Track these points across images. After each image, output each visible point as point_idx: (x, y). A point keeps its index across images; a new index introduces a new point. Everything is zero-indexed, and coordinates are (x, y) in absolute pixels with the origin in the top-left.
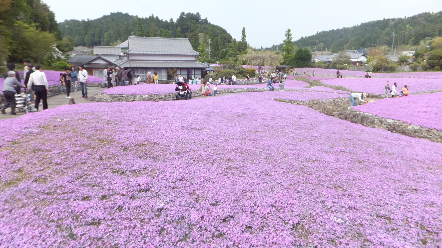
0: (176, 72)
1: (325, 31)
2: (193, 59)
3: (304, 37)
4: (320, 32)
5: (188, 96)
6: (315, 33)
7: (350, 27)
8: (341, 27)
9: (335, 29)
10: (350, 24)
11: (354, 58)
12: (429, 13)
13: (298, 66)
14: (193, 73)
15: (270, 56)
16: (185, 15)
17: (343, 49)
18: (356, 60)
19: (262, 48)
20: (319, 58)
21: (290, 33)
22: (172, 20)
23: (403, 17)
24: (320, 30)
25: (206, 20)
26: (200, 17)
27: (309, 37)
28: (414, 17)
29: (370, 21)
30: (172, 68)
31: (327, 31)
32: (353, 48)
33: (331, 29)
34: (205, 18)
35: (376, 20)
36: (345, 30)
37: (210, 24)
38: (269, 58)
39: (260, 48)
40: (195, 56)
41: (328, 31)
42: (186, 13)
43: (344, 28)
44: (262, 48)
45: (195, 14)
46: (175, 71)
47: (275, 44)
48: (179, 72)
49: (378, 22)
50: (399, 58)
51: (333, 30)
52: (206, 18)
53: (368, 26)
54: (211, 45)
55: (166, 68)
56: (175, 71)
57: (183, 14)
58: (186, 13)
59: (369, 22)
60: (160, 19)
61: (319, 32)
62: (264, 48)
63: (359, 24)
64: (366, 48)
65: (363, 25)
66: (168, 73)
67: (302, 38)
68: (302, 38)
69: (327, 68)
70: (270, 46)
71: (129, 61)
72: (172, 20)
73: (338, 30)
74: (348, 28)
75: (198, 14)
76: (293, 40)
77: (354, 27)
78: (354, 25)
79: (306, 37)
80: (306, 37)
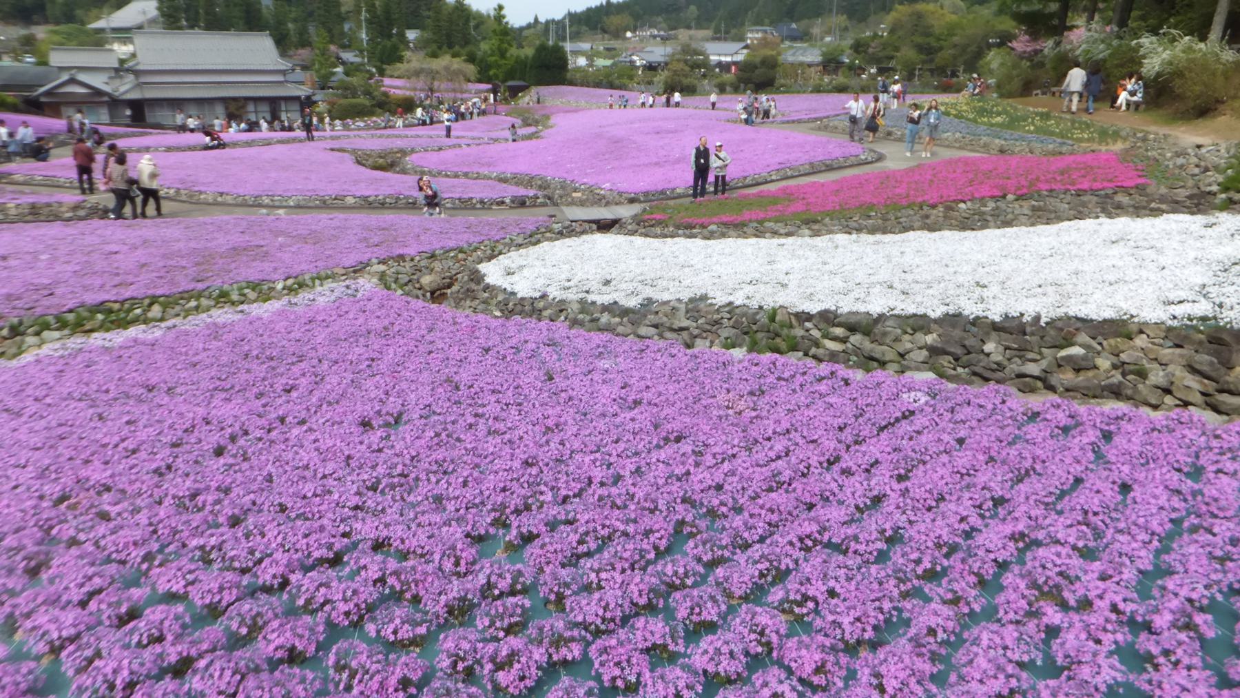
0: (243, 107)
2: (280, 78)
5: (222, 146)
11: (726, 55)
14: (283, 108)
15: (447, 68)
17: (743, 24)
18: (729, 59)
19: (536, 19)
20: (642, 55)
21: (503, 12)
30: (235, 99)
32: (767, 21)
38: (443, 73)
40: (284, 72)
44: (536, 19)
46: (240, 104)
47: (572, 10)
48: (251, 107)
50: (823, 54)
54: (369, 22)
55: (223, 100)
56: (240, 104)
62: (542, 19)
64: (796, 21)
66: (227, 108)
71: (139, 86)
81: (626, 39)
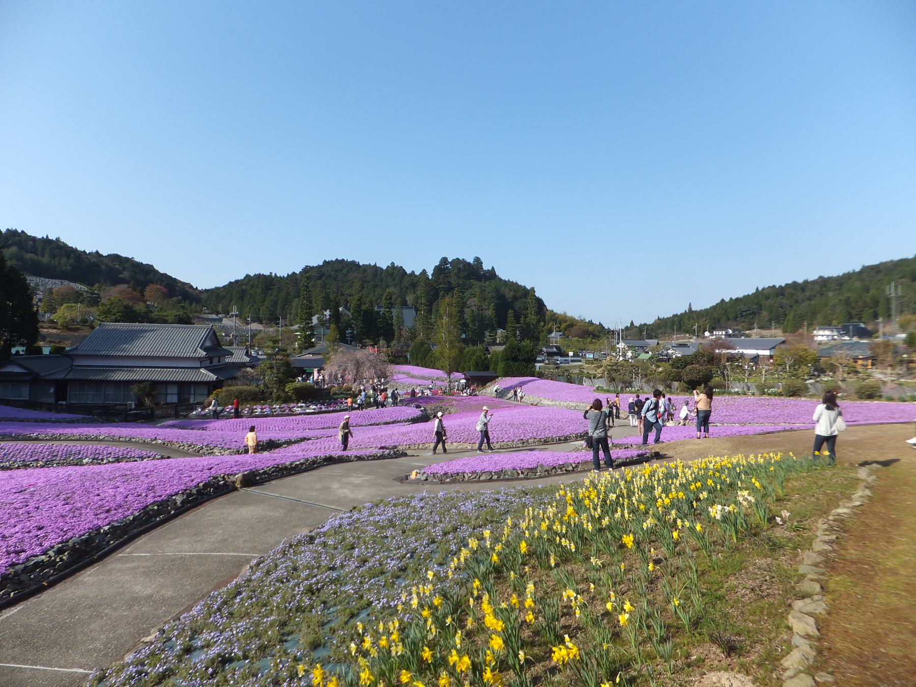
1: (774, 286)
3: (727, 300)
4: (763, 289)
6: (752, 291)
7: (835, 275)
8: (812, 277)
9: (800, 280)
10: (835, 270)
14: (192, 392)
16: (450, 263)
19: (632, 323)
22: (413, 272)
24: (764, 283)
25: (492, 274)
26: (482, 266)
27: (737, 299)
29: (884, 260)
31: (780, 287)
33: (790, 282)
34: (490, 269)
35: (896, 258)
36: (824, 283)
37: (500, 280)
41: (783, 285)
42: (450, 260)
43: (821, 277)
44: (632, 323)
45: (470, 260)
52: (493, 267)
53: (879, 272)
57: (444, 260)
58: (450, 260)
59: (881, 264)
60: (408, 271)
61: (760, 289)
63: (858, 269)
65: (867, 270)
67: (723, 301)
68: (723, 301)
70: (650, 321)
72: (413, 272)
73: (806, 282)
75: (477, 260)
76: (693, 309)
77: (844, 275)
78: (846, 272)
79: (731, 299)
80: (731, 299)
81: (706, 337)
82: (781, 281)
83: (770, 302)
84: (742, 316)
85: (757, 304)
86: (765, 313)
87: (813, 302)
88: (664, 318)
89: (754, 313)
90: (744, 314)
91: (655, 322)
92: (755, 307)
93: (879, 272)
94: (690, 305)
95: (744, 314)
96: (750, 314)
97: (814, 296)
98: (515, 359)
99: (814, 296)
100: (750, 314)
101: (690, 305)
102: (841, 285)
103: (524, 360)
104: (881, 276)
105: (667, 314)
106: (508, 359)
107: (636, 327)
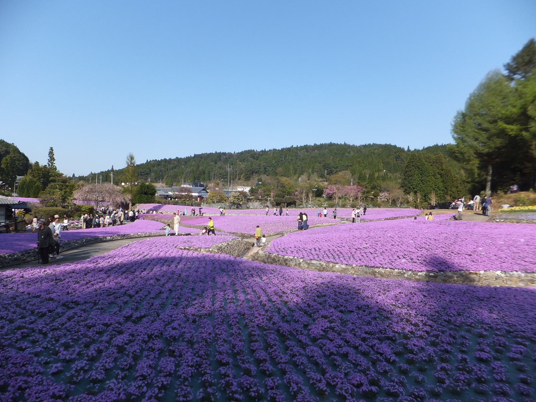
1: (156, 160)
7: (183, 157)
8: (173, 157)
9: (168, 159)
10: (183, 155)
12: (254, 150)
13: (140, 202)
19: (74, 175)
23: (233, 153)
28: (242, 153)
33: (163, 159)
36: (178, 160)
39: (71, 176)
43: (177, 158)
44: (74, 175)
47: (93, 172)
49: (211, 154)
51: (165, 159)
61: (149, 161)
63: (193, 156)
65: (196, 156)
69: (176, 204)
70: (86, 174)
73: (170, 159)
74: (181, 159)
78: (188, 156)
82: (159, 157)
83: (155, 168)
84: (141, 175)
85: (149, 169)
86: (153, 174)
87: (176, 170)
88: (95, 173)
89: (147, 174)
90: (142, 174)
91: (89, 175)
92: (148, 170)
93: (201, 158)
94: (113, 167)
95: (142, 174)
96: (146, 174)
97: (175, 167)
98: (146, 193)
99: (175, 167)
100: (146, 174)
101: (113, 167)
102: (186, 163)
103: (150, 194)
104: (203, 160)
105: (97, 170)
106: (142, 193)
107: (77, 178)
